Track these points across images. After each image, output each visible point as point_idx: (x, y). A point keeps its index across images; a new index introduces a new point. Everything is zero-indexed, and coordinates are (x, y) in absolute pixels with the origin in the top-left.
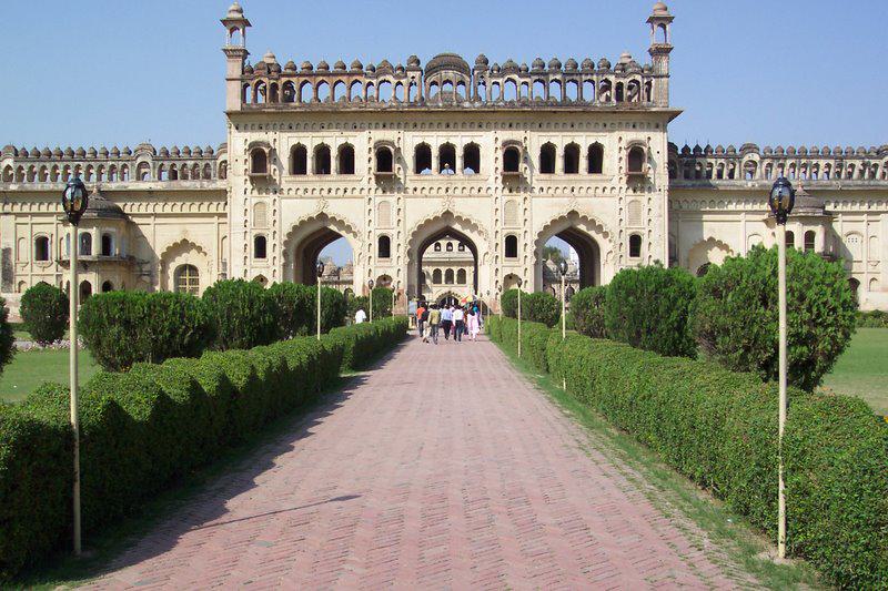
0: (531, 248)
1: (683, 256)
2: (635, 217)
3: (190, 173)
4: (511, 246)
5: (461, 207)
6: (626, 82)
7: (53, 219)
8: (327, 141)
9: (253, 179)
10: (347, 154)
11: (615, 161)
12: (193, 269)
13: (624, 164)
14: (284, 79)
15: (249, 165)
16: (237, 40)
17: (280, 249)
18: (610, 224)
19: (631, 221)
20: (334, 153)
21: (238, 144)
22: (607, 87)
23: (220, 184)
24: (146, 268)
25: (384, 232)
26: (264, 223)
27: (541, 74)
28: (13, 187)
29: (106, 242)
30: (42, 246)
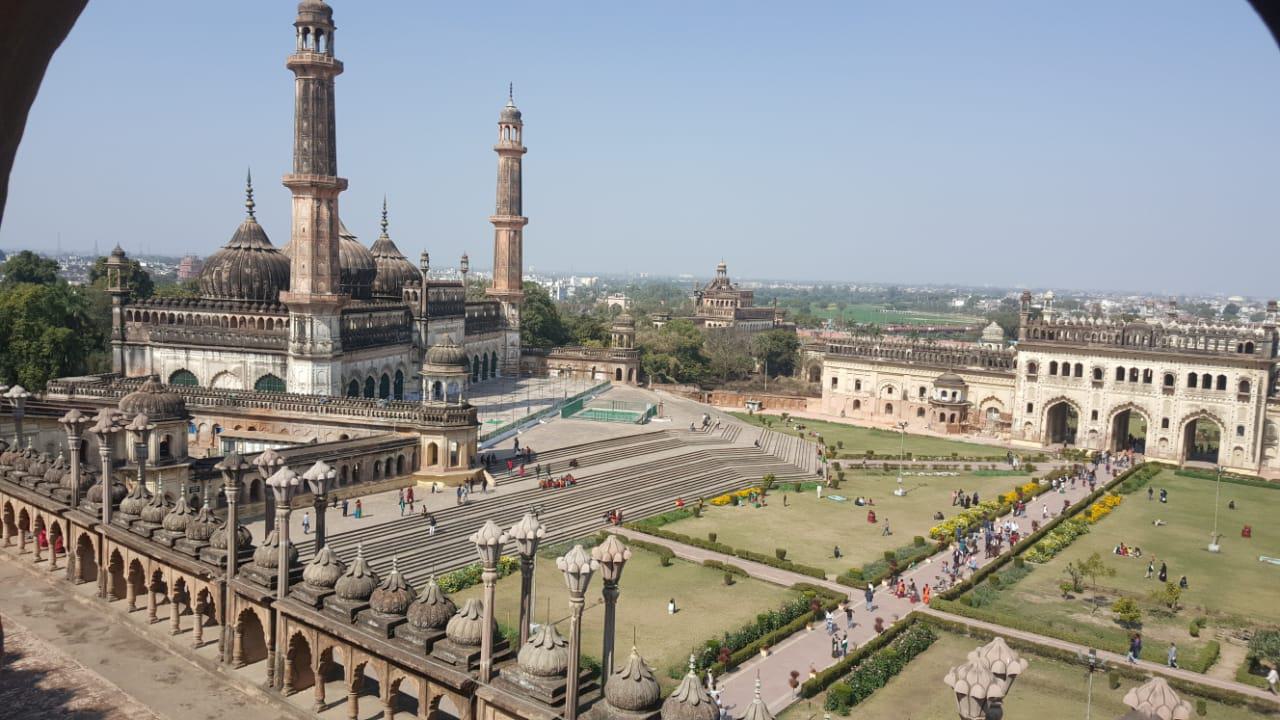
0: (1177, 425)
3: (999, 365)
4: (1165, 423)
5: (1138, 400)
7: (930, 380)
8: (1069, 361)
9: (1029, 377)
10: (1079, 368)
11: (1232, 385)
12: (997, 411)
15: (1026, 369)
17: (1040, 410)
18: (1225, 418)
19: (1239, 418)
20: (1072, 367)
24: (973, 407)
25: (1095, 409)
28: (911, 362)
29: (954, 394)
30: (923, 390)
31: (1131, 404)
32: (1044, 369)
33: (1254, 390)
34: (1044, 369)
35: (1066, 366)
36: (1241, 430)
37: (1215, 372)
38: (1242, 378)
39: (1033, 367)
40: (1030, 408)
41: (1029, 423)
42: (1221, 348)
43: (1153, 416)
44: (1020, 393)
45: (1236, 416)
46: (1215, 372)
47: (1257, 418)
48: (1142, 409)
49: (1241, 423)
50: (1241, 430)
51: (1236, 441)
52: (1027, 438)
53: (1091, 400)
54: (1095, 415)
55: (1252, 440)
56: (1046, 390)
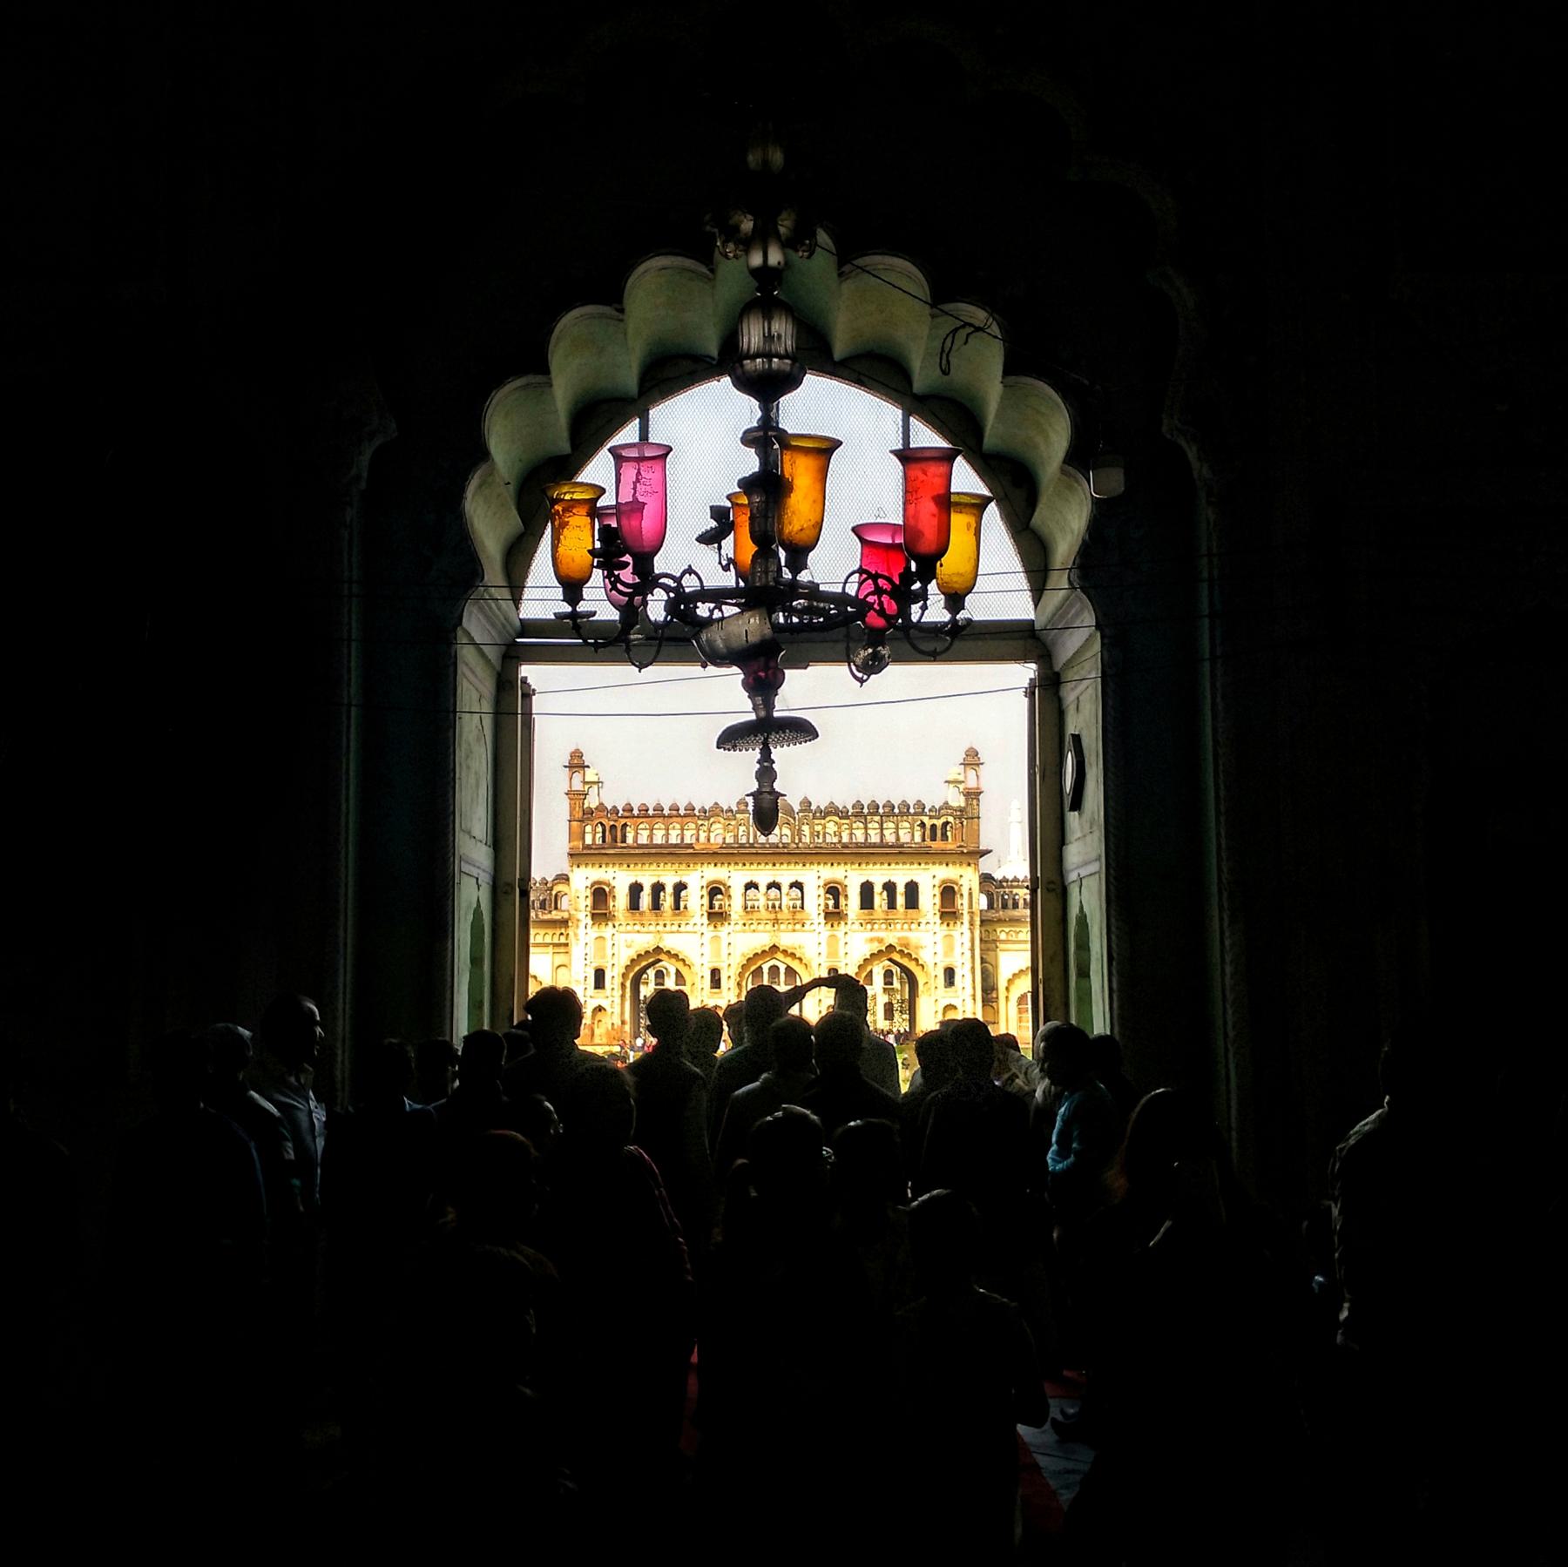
1: (1002, 984)
2: (949, 950)
5: (786, 939)
6: (939, 823)
9: (594, 916)
11: (929, 899)
13: (938, 900)
14: (623, 821)
15: (589, 902)
16: (577, 785)
17: (618, 980)
18: (925, 956)
19: (946, 955)
21: (583, 878)
22: (923, 825)
23: (555, 915)
25: (716, 965)
26: (603, 957)
27: (861, 813)
31: (774, 948)
32: (621, 901)
33: (962, 903)
34: (621, 901)
35: (658, 888)
36: (950, 974)
37: (901, 875)
38: (944, 882)
39: (600, 895)
40: (600, 975)
41: (600, 1009)
42: (905, 837)
43: (814, 965)
44: (577, 949)
45: (940, 949)
46: (901, 875)
47: (972, 950)
48: (793, 955)
49: (947, 962)
50: (950, 974)
51: (947, 996)
52: (597, 1040)
53: (707, 950)
54: (715, 973)
55: (969, 991)
56: (625, 941)
